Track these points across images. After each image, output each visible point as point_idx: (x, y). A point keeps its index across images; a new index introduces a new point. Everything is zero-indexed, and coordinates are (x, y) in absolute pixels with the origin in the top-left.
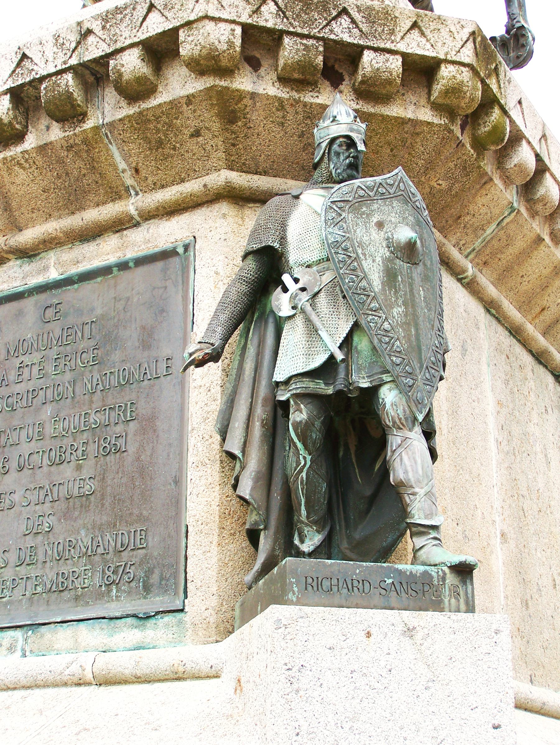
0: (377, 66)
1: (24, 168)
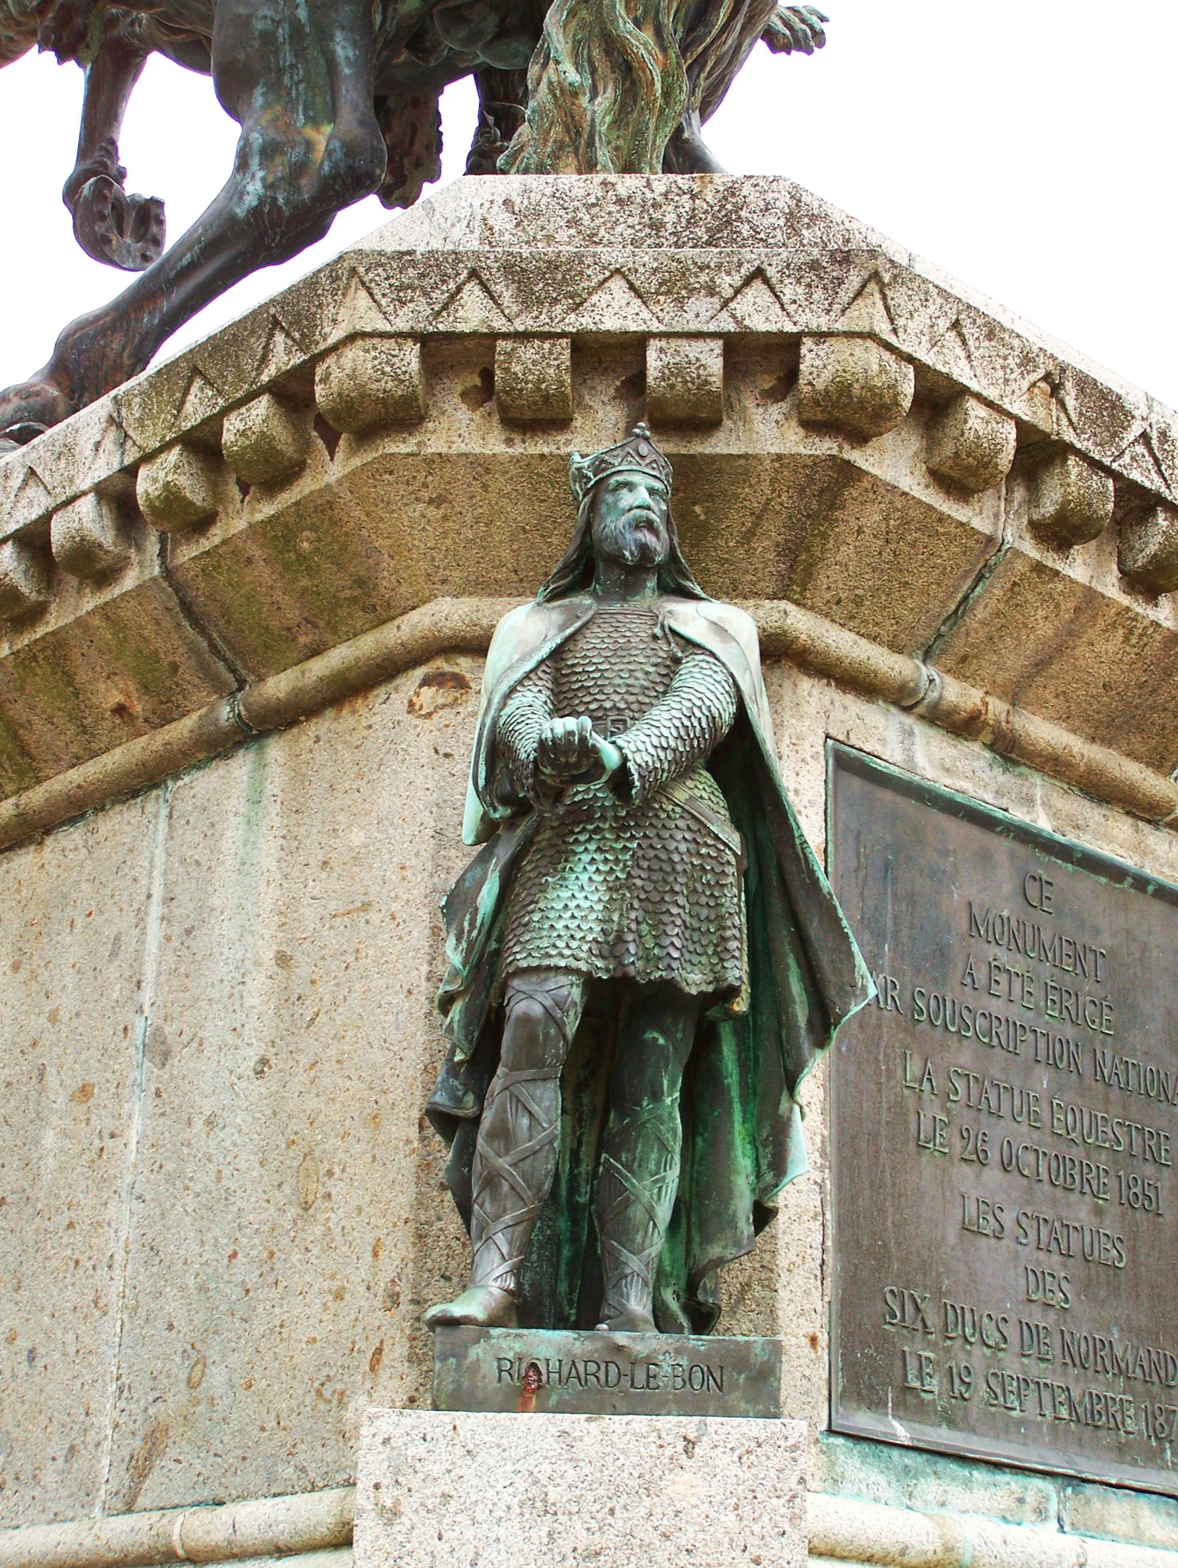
1: (1126, 639)
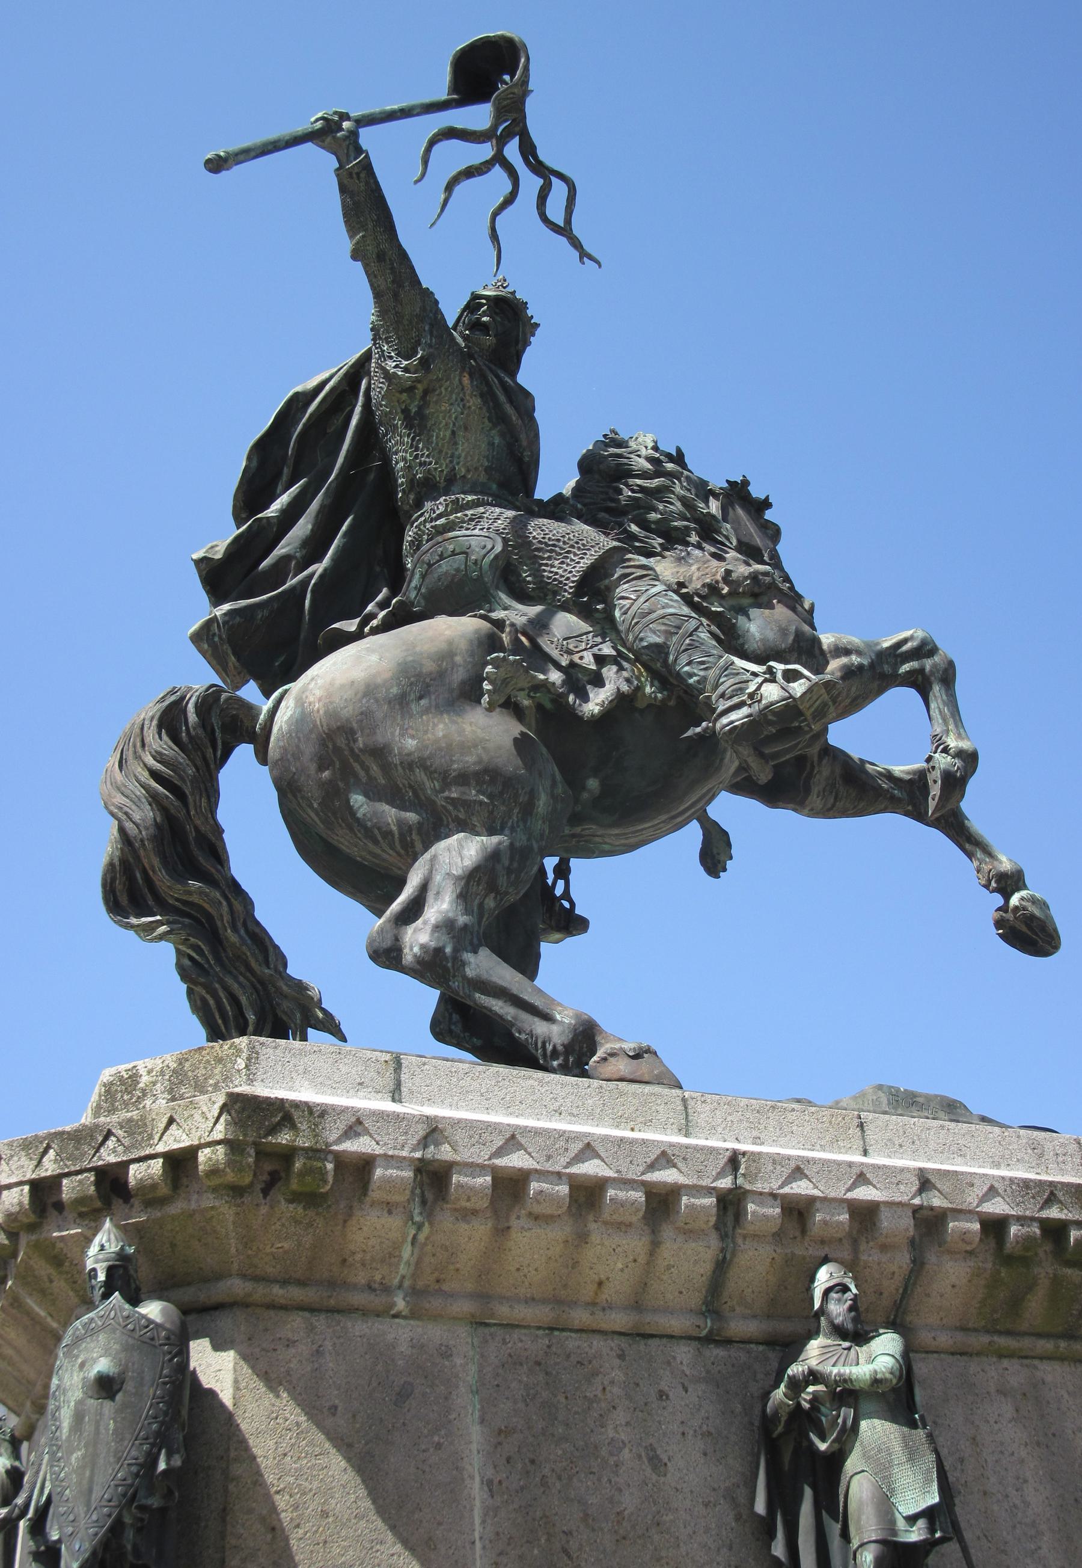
0: (139, 1176)
